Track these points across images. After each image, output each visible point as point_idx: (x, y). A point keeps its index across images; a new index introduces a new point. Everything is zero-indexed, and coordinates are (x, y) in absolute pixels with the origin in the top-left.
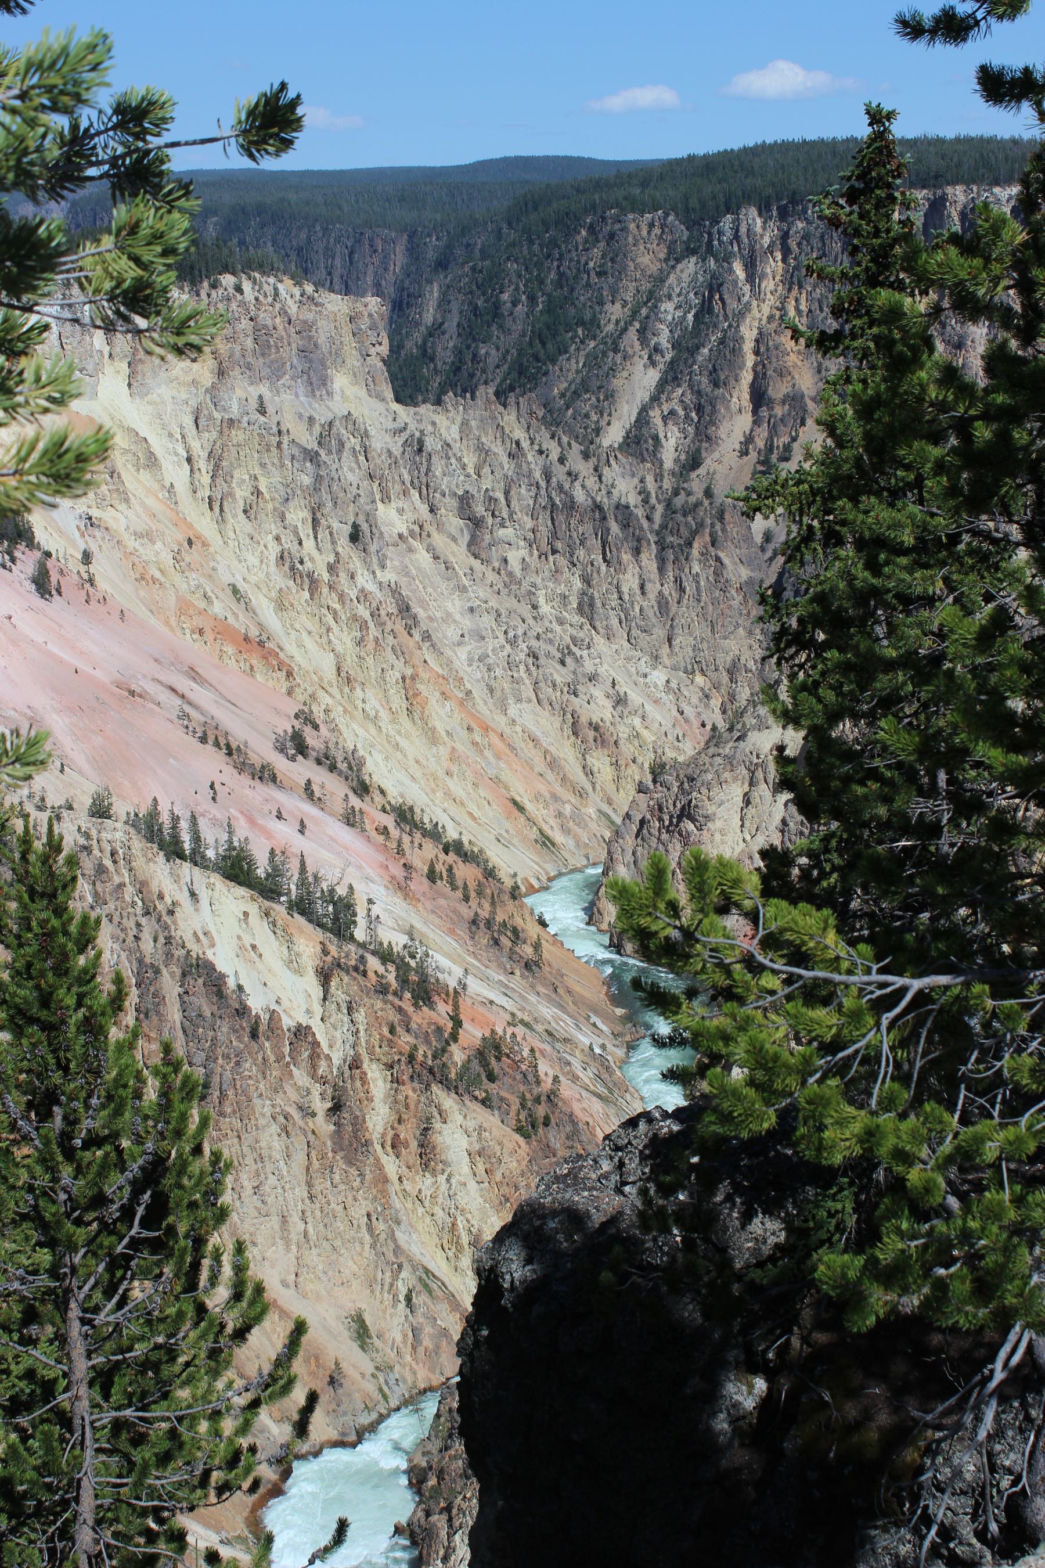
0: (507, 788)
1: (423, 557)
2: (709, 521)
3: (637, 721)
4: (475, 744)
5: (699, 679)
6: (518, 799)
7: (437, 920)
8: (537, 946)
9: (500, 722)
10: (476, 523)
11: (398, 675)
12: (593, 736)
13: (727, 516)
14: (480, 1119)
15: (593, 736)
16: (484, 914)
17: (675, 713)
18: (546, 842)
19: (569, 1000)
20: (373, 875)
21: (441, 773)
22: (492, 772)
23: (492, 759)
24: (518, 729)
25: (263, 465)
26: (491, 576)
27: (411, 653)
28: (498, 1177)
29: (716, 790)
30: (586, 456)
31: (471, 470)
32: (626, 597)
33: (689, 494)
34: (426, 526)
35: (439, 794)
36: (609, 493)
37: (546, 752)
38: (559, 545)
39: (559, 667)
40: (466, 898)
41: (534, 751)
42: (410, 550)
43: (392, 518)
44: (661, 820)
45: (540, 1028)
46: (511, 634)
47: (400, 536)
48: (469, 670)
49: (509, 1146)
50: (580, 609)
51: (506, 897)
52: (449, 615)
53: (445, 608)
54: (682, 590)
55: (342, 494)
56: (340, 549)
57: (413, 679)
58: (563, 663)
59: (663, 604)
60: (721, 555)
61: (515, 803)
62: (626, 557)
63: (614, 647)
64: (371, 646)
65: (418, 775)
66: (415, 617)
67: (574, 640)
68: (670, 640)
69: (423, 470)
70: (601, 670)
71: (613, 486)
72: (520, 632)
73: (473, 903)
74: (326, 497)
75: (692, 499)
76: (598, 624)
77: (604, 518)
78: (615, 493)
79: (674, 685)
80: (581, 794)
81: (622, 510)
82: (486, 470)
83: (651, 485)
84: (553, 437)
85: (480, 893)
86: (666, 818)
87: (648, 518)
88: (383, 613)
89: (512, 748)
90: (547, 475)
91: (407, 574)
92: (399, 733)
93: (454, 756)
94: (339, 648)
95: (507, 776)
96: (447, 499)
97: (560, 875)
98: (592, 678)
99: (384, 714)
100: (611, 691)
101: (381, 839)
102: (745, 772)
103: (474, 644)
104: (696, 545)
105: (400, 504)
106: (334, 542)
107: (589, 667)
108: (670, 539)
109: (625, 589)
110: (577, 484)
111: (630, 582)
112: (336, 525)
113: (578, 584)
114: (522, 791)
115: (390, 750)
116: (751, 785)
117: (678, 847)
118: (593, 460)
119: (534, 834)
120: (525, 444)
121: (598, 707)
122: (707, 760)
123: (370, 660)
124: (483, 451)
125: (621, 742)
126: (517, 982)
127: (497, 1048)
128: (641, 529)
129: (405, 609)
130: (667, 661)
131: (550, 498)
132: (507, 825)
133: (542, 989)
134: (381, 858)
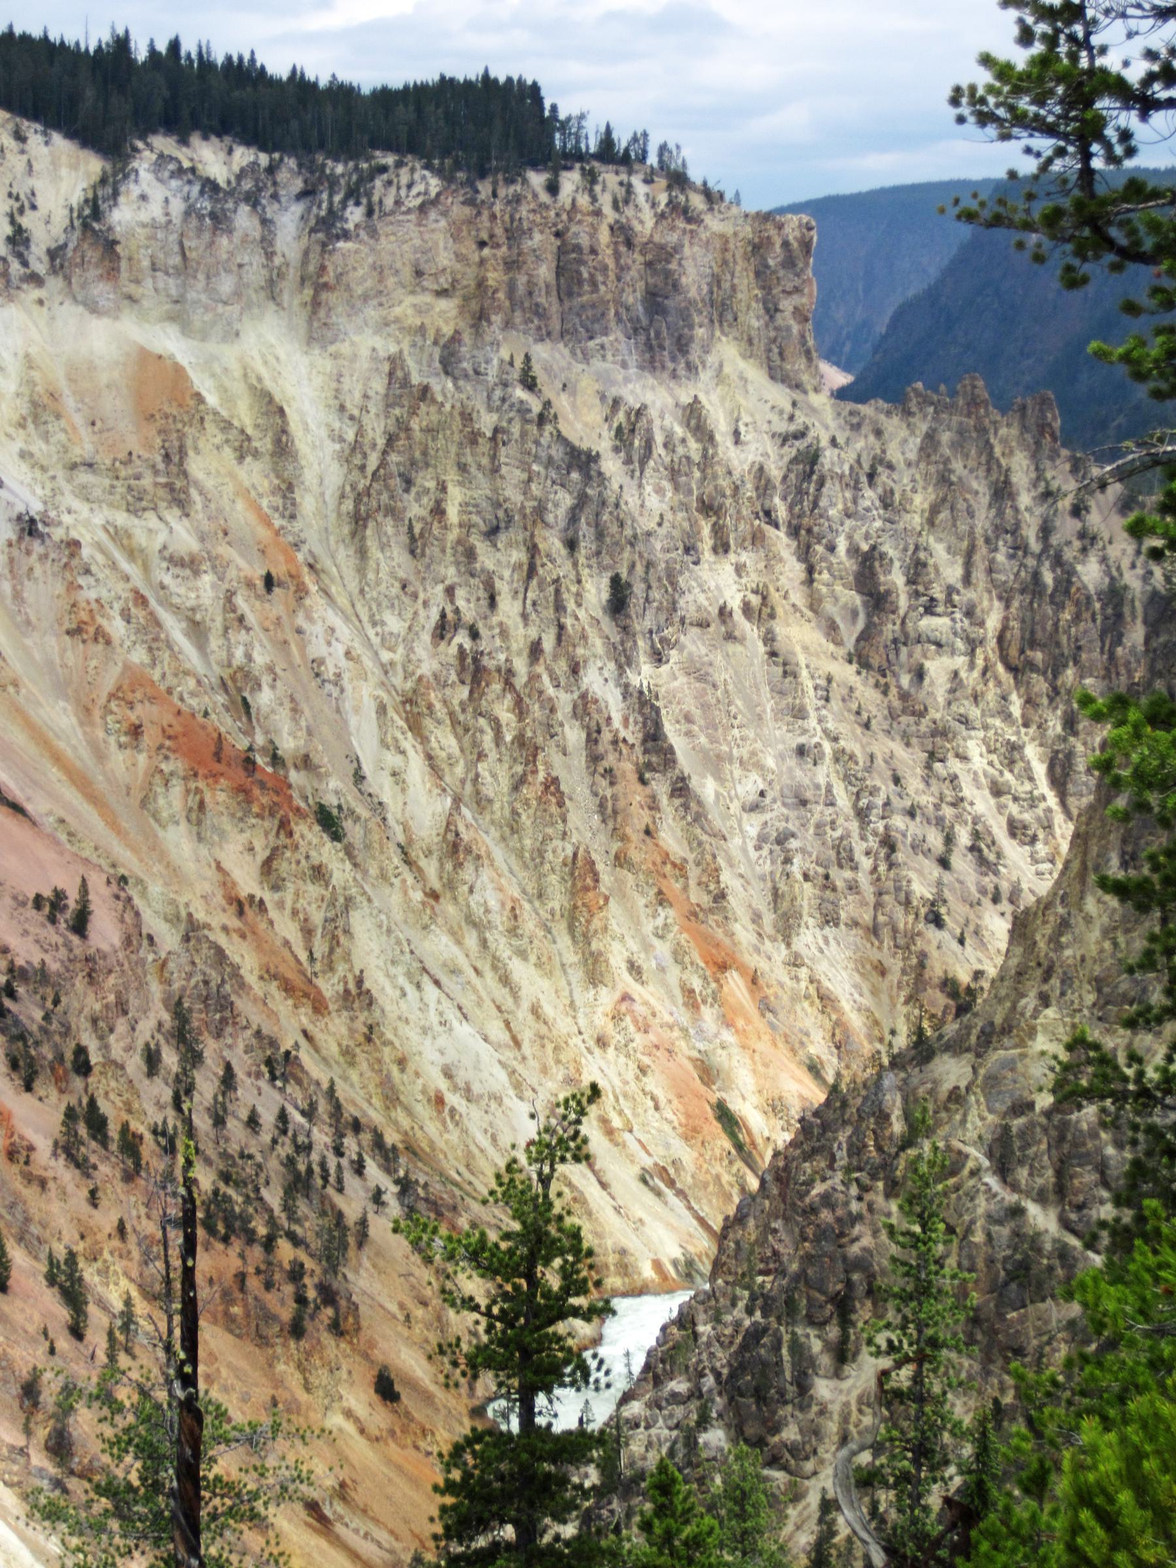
25: (463, 468)
46: (863, 802)
48: (753, 855)
55: (614, 529)
65: (526, 1036)
90: (1046, 531)
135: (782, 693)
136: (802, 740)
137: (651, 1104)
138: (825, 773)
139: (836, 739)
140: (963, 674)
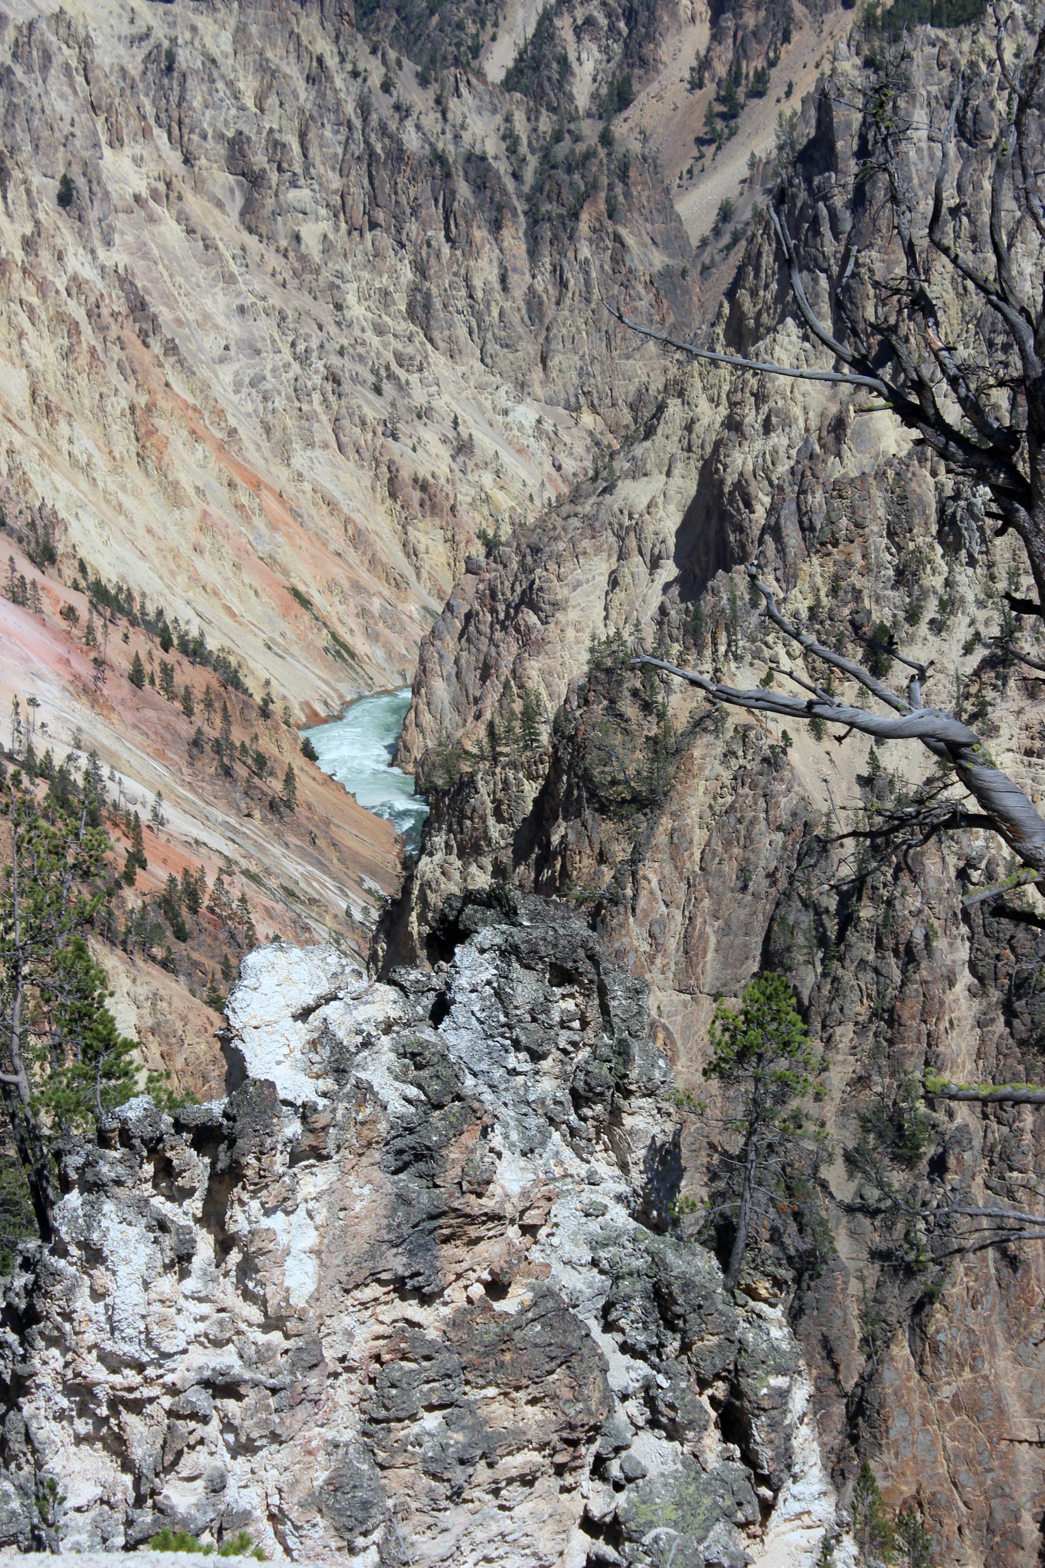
0: (286, 573)
1: (171, 230)
2: (604, 180)
3: (487, 479)
4: (239, 507)
5: (587, 419)
6: (302, 588)
7: (140, 738)
8: (289, 780)
9: (280, 476)
10: (253, 180)
11: (125, 404)
12: (418, 498)
13: (633, 173)
14: (155, 984)
15: (418, 498)
16: (213, 733)
17: (548, 467)
18: (341, 652)
19: (334, 856)
20: (45, 670)
21: (186, 549)
22: (264, 549)
23: (264, 530)
24: (307, 487)
26: (273, 260)
27: (147, 373)
28: (179, 1063)
29: (570, 565)
30: (424, 81)
31: (250, 103)
32: (479, 294)
33: (577, 139)
34: (177, 184)
35: (182, 579)
36: (457, 137)
37: (347, 521)
38: (380, 216)
39: (371, 396)
40: (188, 712)
41: (329, 520)
42: (152, 219)
43: (125, 171)
44: (493, 611)
45: (273, 883)
46: (301, 347)
47: (137, 198)
48: (235, 398)
49: (196, 1021)
50: (411, 314)
51: (254, 715)
52: (207, 317)
53: (204, 308)
54: (563, 284)
55: (47, 133)
56: (41, 216)
57: (149, 409)
58: (378, 390)
59: (534, 305)
60: (623, 232)
61: (296, 594)
62: (480, 234)
63: (460, 369)
64: (84, 360)
65: (150, 550)
66: (154, 319)
67: (399, 358)
68: (544, 360)
69: (174, 99)
70: (438, 403)
71: (463, 127)
72: (314, 344)
73: (198, 719)
74: (22, 136)
75: (581, 148)
76: (436, 335)
77: (448, 175)
78: (467, 137)
79: (548, 426)
80: (398, 584)
81: (476, 161)
82: (272, 100)
83: (521, 125)
84: (374, 52)
85: (209, 705)
86: (501, 608)
87: (516, 176)
88: (105, 312)
89: (296, 515)
90: (364, 108)
91: (146, 256)
92: (123, 488)
93: (206, 523)
94: (37, 363)
95: (286, 555)
96: (210, 144)
97: (361, 698)
98: (423, 414)
99: (100, 460)
100: (451, 434)
101: (64, 624)
102: (612, 539)
103: (244, 361)
104: (584, 216)
105: (138, 150)
106: (32, 205)
107: (419, 396)
108: (546, 207)
109: (477, 282)
110: (409, 124)
111: (485, 272)
112: (36, 180)
113: (407, 274)
114: (309, 579)
115: (109, 512)
116: (620, 558)
117: (514, 648)
118: (434, 89)
119: (323, 639)
120: (332, 62)
121: (429, 456)
122: (559, 522)
123: (82, 381)
124: (266, 70)
125: (462, 509)
126: (255, 827)
127: (193, 895)
128: (504, 192)
129: (138, 307)
130: (539, 391)
131: (367, 143)
132: (283, 625)
133: (292, 840)
134: (61, 649)
135: (208, 264)
136: (239, 301)
137: (252, 593)
138: (265, 327)
139: (264, 299)
140: (331, 236)
